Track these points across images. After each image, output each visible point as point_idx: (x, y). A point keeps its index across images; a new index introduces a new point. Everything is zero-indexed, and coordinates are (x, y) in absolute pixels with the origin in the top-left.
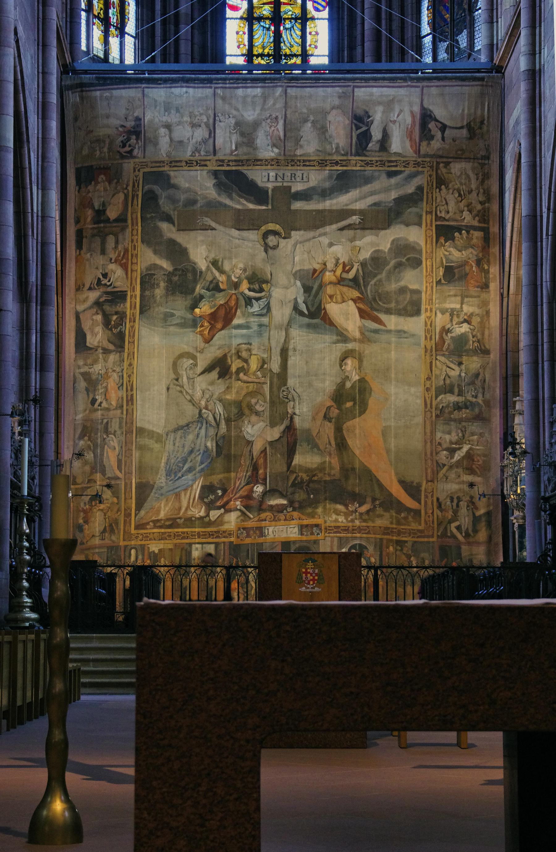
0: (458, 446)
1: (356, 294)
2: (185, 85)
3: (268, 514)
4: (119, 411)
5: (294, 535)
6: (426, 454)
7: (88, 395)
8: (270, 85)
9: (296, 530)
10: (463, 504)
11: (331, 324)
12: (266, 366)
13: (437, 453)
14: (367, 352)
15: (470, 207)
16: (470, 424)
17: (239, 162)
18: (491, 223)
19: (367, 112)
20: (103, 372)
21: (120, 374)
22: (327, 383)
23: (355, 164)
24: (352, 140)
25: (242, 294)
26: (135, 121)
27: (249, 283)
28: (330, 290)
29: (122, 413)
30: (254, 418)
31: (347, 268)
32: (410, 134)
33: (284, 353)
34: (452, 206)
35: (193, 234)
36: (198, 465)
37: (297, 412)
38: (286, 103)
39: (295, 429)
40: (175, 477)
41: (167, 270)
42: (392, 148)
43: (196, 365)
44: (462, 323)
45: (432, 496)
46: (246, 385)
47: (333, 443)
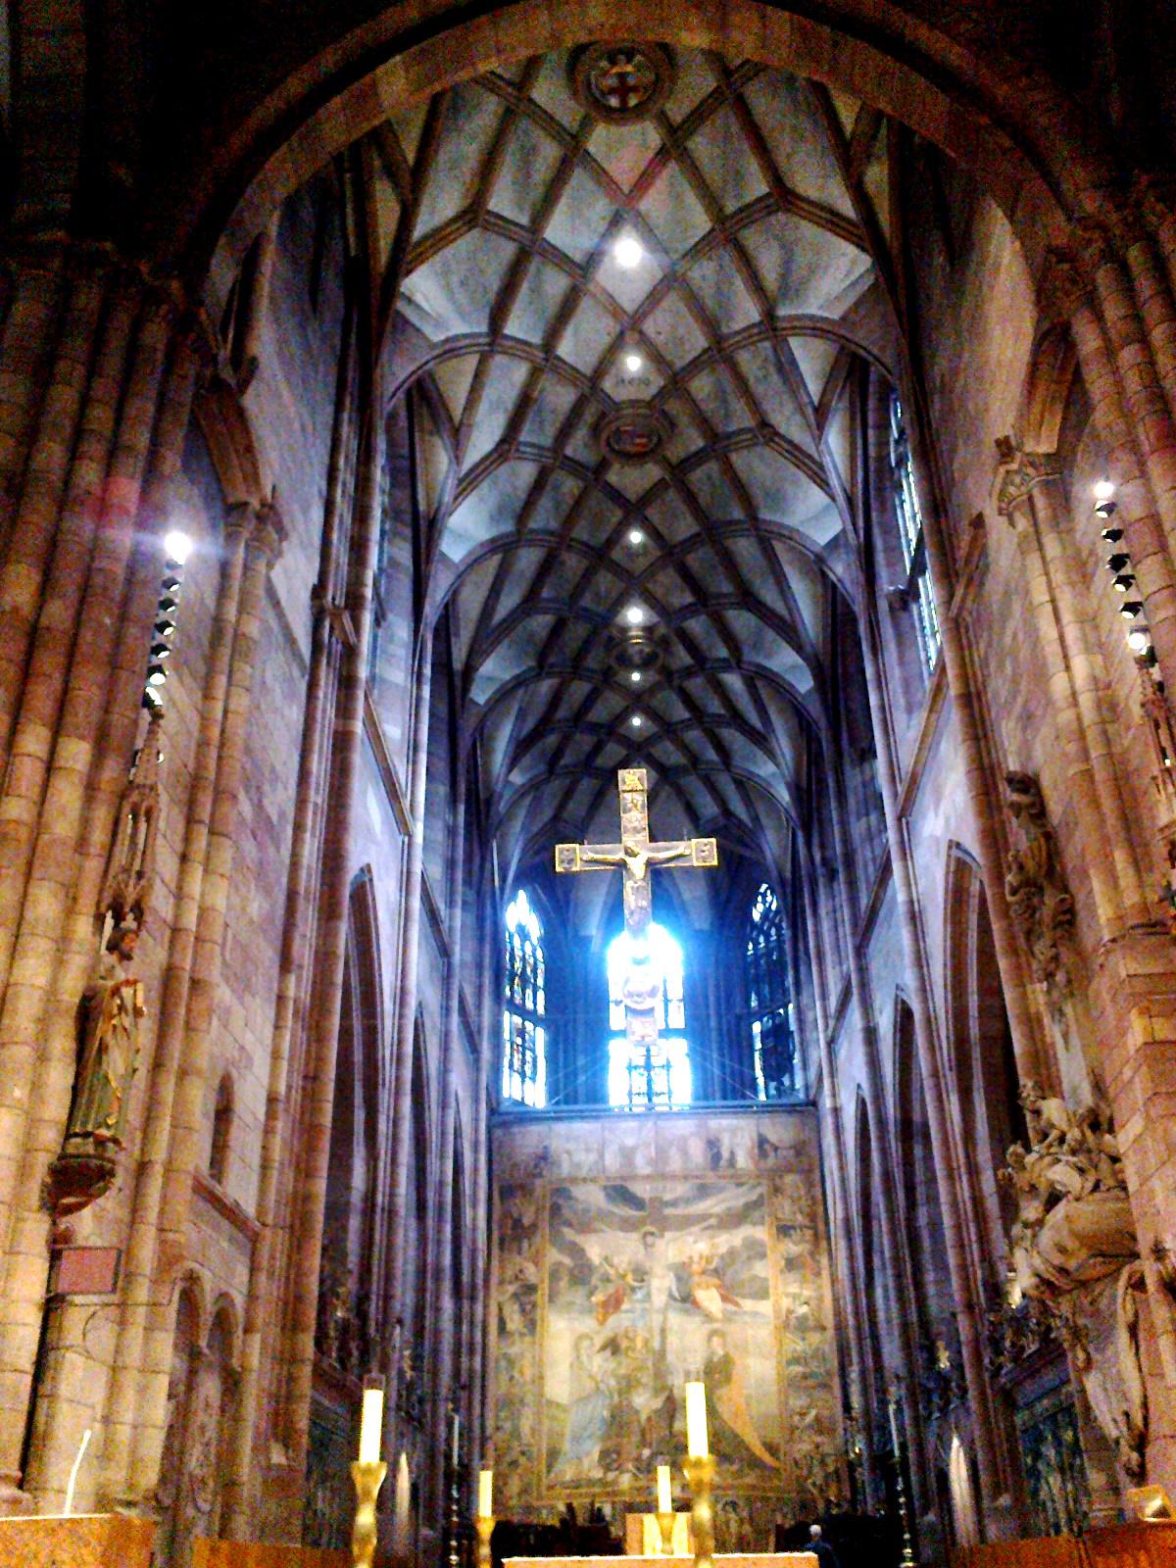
1: (716, 1281)
17: (622, 1178)
28: (696, 1279)
33: (663, 1331)
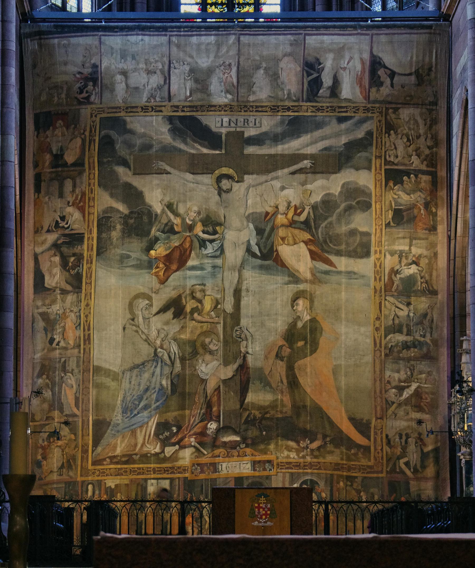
0: (406, 384)
1: (307, 236)
2: (140, 33)
3: (221, 450)
4: (76, 351)
5: (247, 471)
7: (46, 334)
8: (224, 33)
9: (249, 466)
11: (283, 265)
12: (219, 306)
13: (386, 391)
14: (318, 293)
15: (418, 152)
16: (418, 362)
17: (193, 108)
18: (439, 167)
20: (61, 312)
21: (78, 314)
22: (279, 323)
23: (307, 110)
25: (196, 236)
26: (92, 68)
27: (203, 226)
28: (281, 232)
30: (208, 357)
31: (299, 211)
33: (237, 293)
34: (401, 151)
35: (148, 178)
36: (153, 402)
37: (250, 351)
38: (239, 50)
40: (131, 414)
41: (123, 213)
42: (342, 94)
43: (151, 305)
44: (411, 264)
45: (382, 433)
46: (200, 324)
47: (285, 381)
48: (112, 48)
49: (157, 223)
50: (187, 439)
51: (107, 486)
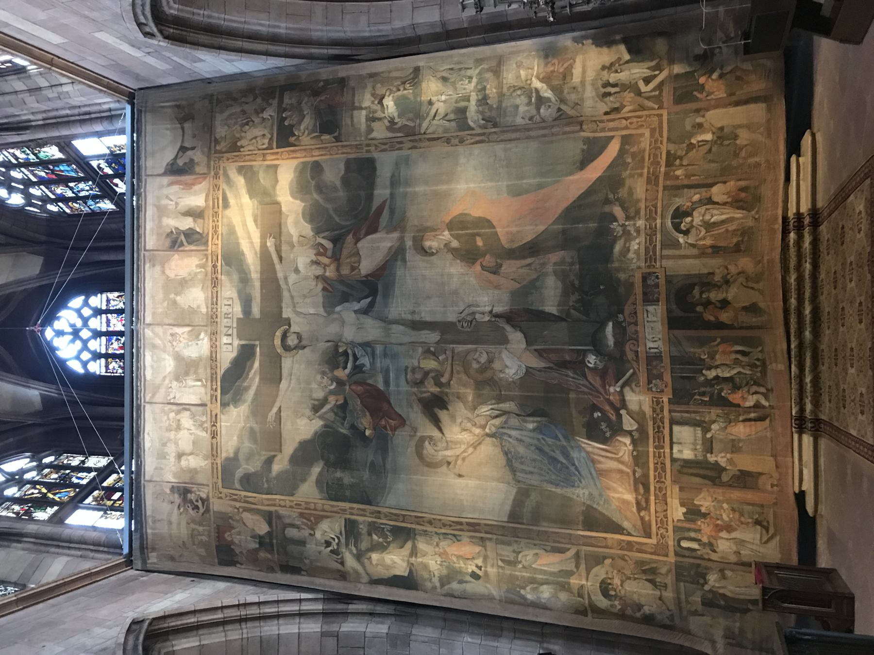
0: (534, 95)
1: (350, 239)
3: (627, 348)
5: (659, 311)
6: (544, 136)
7: (466, 582)
10: (613, 78)
12: (432, 349)
13: (544, 121)
16: (505, 82)
17: (213, 378)
19: (168, 235)
20: (439, 560)
22: (453, 270)
23: (216, 246)
24: (192, 251)
25: (350, 376)
28: (345, 271)
29: (490, 539)
30: (497, 365)
31: (321, 250)
32: (189, 186)
33: (417, 325)
36: (558, 443)
37: (488, 309)
38: (158, 325)
39: (511, 312)
40: (575, 475)
44: (382, 105)
45: (602, 121)
46: (455, 375)
47: (529, 261)
48: (156, 469)
49: (334, 426)
50: (611, 398)
51: (683, 518)
